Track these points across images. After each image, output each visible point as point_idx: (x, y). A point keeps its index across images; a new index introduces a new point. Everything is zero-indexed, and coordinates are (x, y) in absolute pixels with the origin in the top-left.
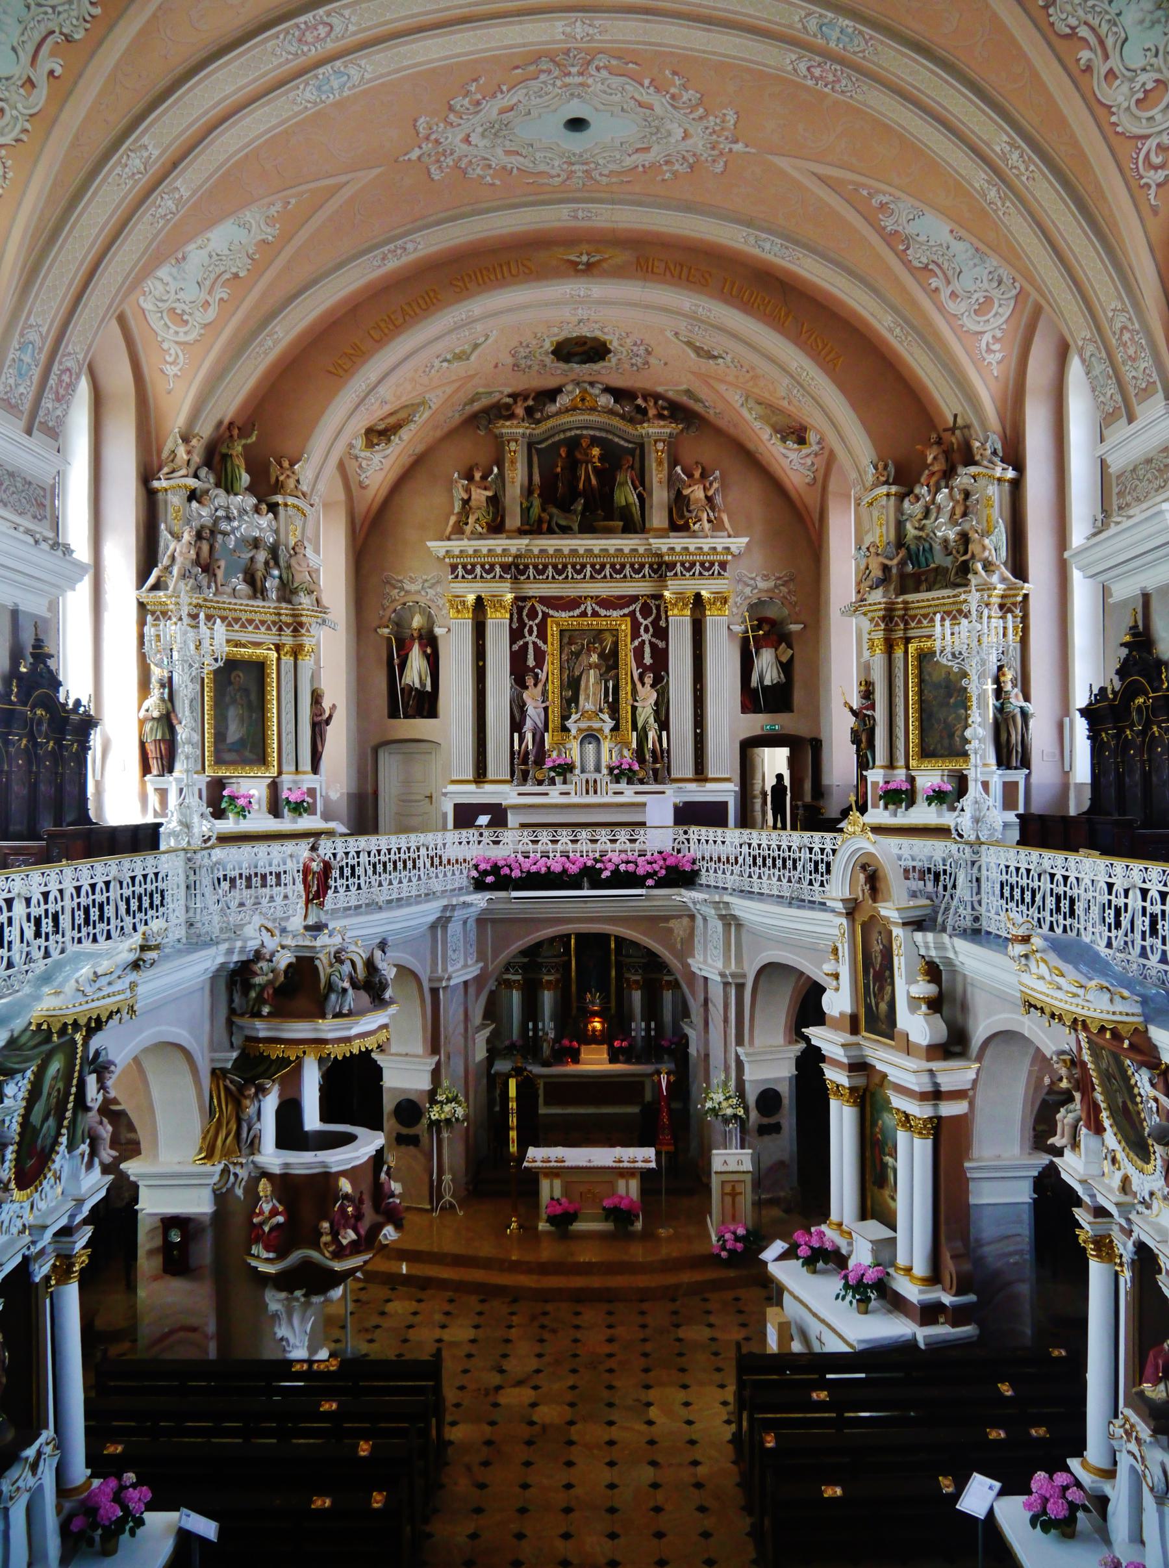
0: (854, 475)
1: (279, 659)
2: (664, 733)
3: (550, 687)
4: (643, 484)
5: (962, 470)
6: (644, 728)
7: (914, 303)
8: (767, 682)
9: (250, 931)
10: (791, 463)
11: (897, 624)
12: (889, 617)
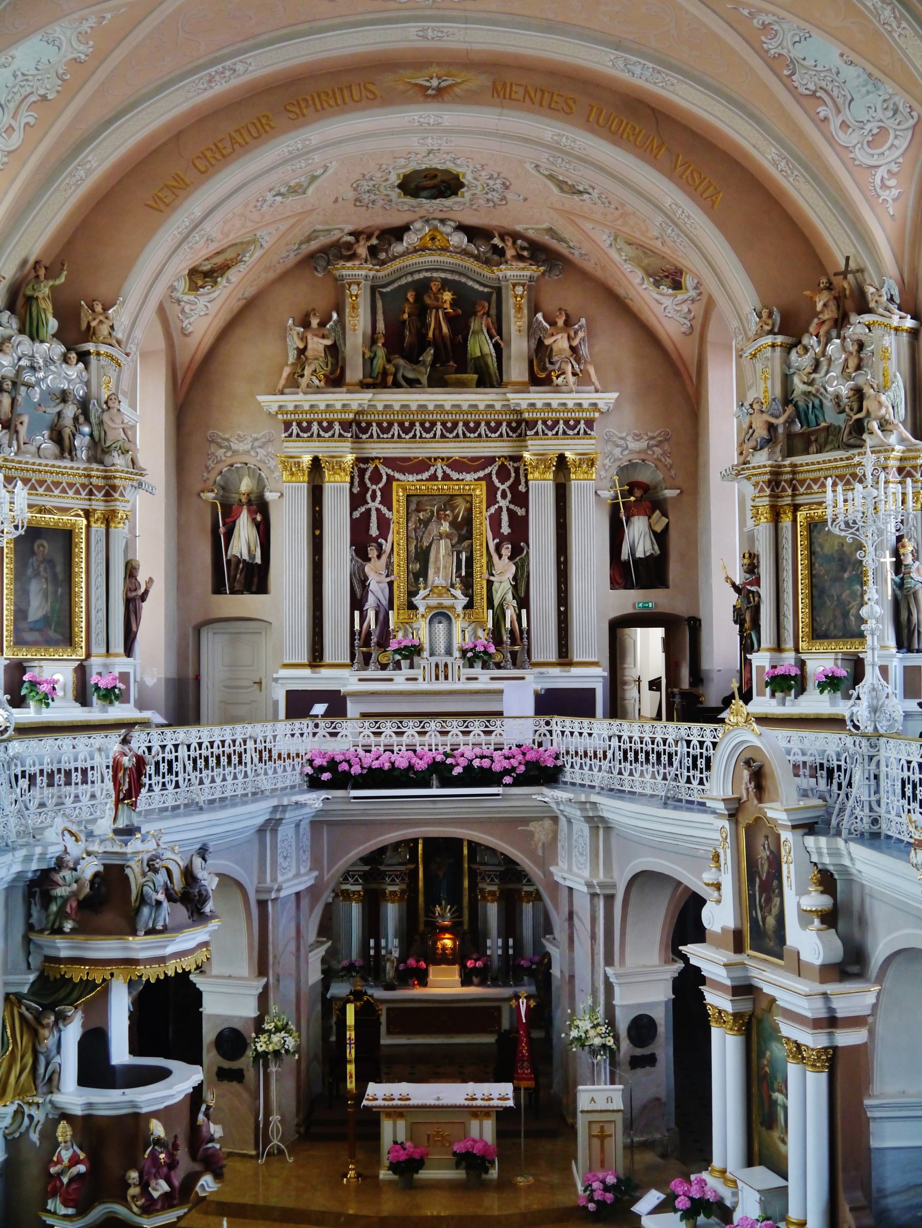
0: (735, 323)
1: (88, 526)
2: (524, 612)
3: (395, 559)
4: (500, 333)
5: (854, 318)
6: (501, 605)
7: (800, 134)
8: (640, 554)
9: (51, 835)
10: (665, 311)
11: (784, 490)
12: (775, 482)
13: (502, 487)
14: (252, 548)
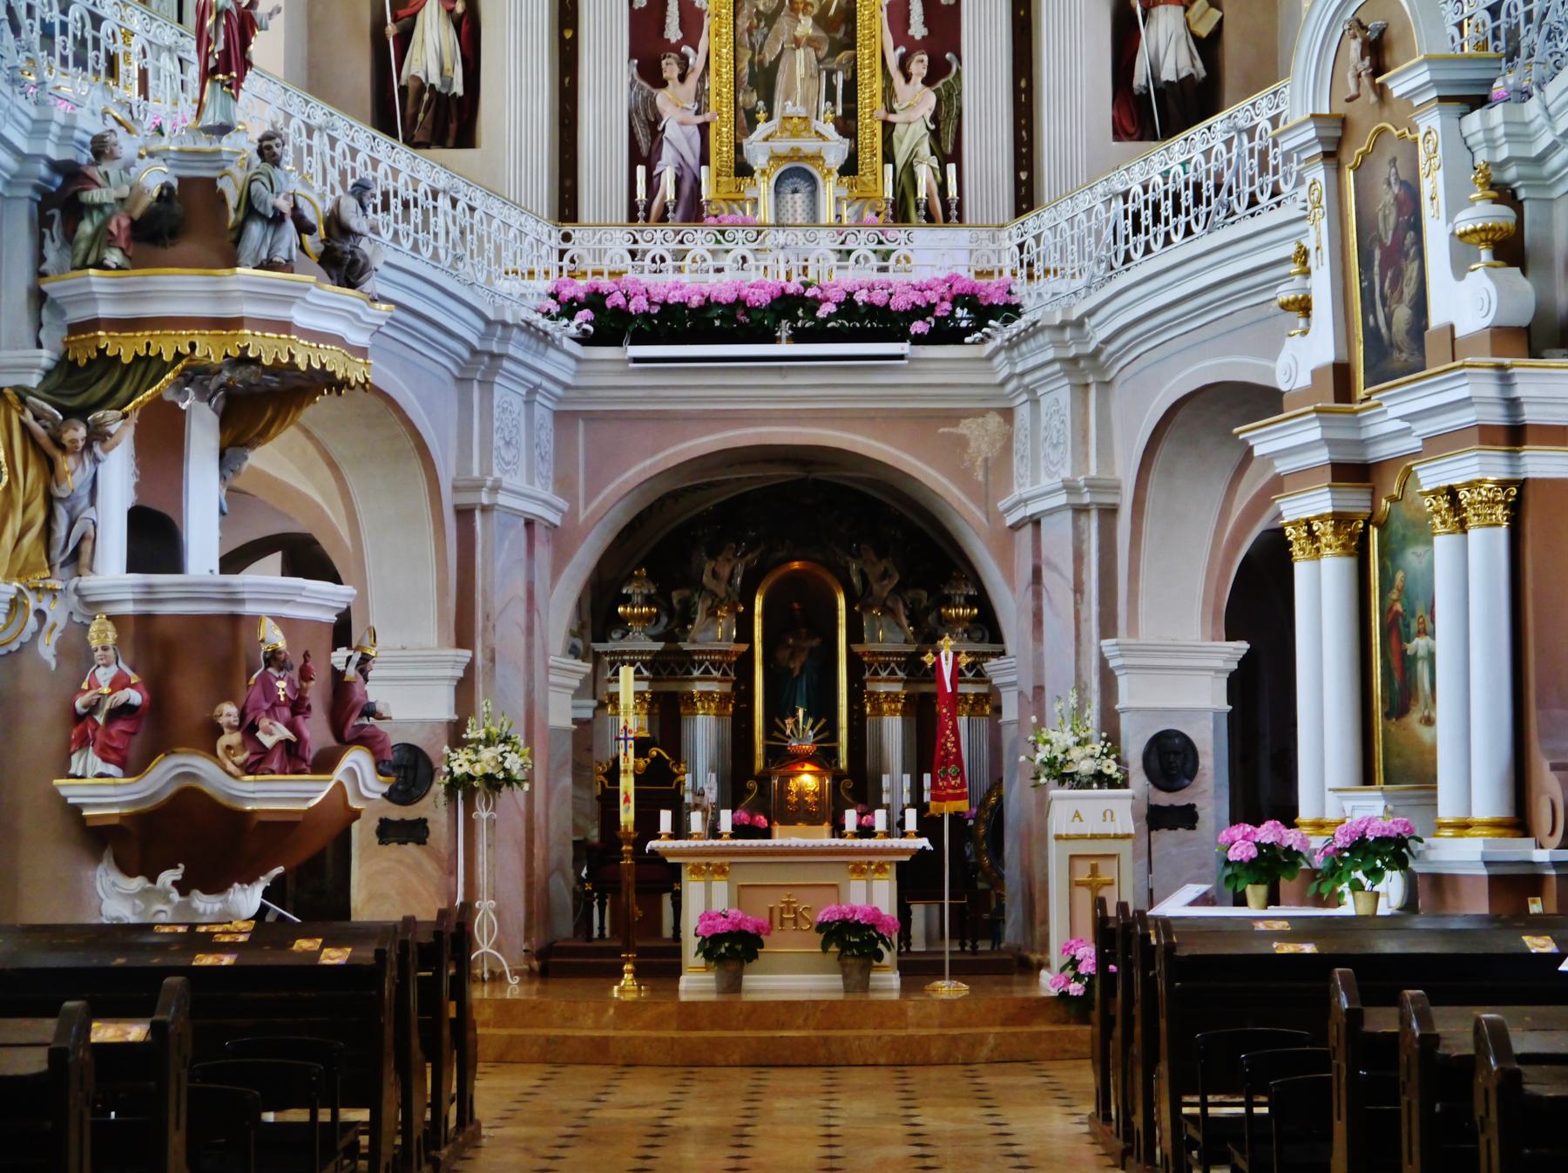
2: (951, 168)
3: (712, 83)
6: (910, 168)
8: (1168, 75)
14: (448, 65)
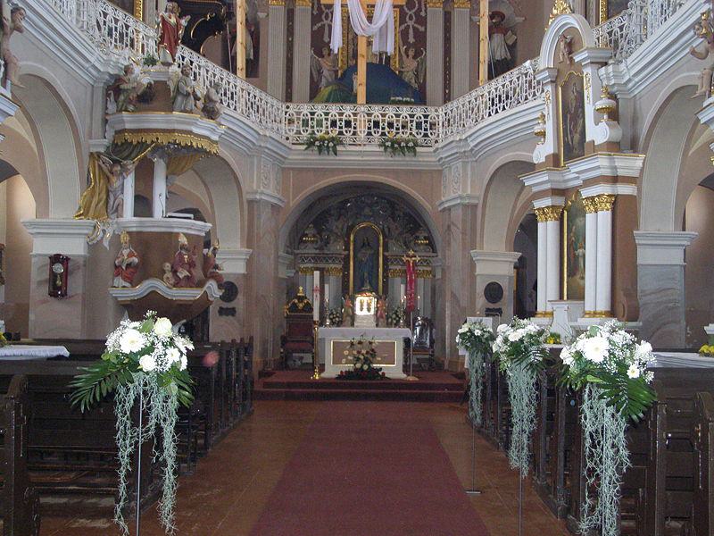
8: (498, 57)
13: (410, 13)
